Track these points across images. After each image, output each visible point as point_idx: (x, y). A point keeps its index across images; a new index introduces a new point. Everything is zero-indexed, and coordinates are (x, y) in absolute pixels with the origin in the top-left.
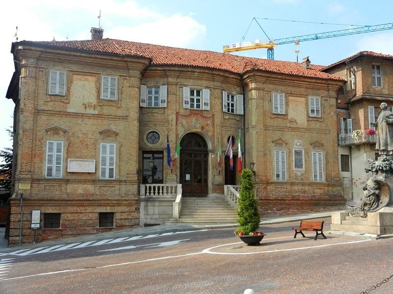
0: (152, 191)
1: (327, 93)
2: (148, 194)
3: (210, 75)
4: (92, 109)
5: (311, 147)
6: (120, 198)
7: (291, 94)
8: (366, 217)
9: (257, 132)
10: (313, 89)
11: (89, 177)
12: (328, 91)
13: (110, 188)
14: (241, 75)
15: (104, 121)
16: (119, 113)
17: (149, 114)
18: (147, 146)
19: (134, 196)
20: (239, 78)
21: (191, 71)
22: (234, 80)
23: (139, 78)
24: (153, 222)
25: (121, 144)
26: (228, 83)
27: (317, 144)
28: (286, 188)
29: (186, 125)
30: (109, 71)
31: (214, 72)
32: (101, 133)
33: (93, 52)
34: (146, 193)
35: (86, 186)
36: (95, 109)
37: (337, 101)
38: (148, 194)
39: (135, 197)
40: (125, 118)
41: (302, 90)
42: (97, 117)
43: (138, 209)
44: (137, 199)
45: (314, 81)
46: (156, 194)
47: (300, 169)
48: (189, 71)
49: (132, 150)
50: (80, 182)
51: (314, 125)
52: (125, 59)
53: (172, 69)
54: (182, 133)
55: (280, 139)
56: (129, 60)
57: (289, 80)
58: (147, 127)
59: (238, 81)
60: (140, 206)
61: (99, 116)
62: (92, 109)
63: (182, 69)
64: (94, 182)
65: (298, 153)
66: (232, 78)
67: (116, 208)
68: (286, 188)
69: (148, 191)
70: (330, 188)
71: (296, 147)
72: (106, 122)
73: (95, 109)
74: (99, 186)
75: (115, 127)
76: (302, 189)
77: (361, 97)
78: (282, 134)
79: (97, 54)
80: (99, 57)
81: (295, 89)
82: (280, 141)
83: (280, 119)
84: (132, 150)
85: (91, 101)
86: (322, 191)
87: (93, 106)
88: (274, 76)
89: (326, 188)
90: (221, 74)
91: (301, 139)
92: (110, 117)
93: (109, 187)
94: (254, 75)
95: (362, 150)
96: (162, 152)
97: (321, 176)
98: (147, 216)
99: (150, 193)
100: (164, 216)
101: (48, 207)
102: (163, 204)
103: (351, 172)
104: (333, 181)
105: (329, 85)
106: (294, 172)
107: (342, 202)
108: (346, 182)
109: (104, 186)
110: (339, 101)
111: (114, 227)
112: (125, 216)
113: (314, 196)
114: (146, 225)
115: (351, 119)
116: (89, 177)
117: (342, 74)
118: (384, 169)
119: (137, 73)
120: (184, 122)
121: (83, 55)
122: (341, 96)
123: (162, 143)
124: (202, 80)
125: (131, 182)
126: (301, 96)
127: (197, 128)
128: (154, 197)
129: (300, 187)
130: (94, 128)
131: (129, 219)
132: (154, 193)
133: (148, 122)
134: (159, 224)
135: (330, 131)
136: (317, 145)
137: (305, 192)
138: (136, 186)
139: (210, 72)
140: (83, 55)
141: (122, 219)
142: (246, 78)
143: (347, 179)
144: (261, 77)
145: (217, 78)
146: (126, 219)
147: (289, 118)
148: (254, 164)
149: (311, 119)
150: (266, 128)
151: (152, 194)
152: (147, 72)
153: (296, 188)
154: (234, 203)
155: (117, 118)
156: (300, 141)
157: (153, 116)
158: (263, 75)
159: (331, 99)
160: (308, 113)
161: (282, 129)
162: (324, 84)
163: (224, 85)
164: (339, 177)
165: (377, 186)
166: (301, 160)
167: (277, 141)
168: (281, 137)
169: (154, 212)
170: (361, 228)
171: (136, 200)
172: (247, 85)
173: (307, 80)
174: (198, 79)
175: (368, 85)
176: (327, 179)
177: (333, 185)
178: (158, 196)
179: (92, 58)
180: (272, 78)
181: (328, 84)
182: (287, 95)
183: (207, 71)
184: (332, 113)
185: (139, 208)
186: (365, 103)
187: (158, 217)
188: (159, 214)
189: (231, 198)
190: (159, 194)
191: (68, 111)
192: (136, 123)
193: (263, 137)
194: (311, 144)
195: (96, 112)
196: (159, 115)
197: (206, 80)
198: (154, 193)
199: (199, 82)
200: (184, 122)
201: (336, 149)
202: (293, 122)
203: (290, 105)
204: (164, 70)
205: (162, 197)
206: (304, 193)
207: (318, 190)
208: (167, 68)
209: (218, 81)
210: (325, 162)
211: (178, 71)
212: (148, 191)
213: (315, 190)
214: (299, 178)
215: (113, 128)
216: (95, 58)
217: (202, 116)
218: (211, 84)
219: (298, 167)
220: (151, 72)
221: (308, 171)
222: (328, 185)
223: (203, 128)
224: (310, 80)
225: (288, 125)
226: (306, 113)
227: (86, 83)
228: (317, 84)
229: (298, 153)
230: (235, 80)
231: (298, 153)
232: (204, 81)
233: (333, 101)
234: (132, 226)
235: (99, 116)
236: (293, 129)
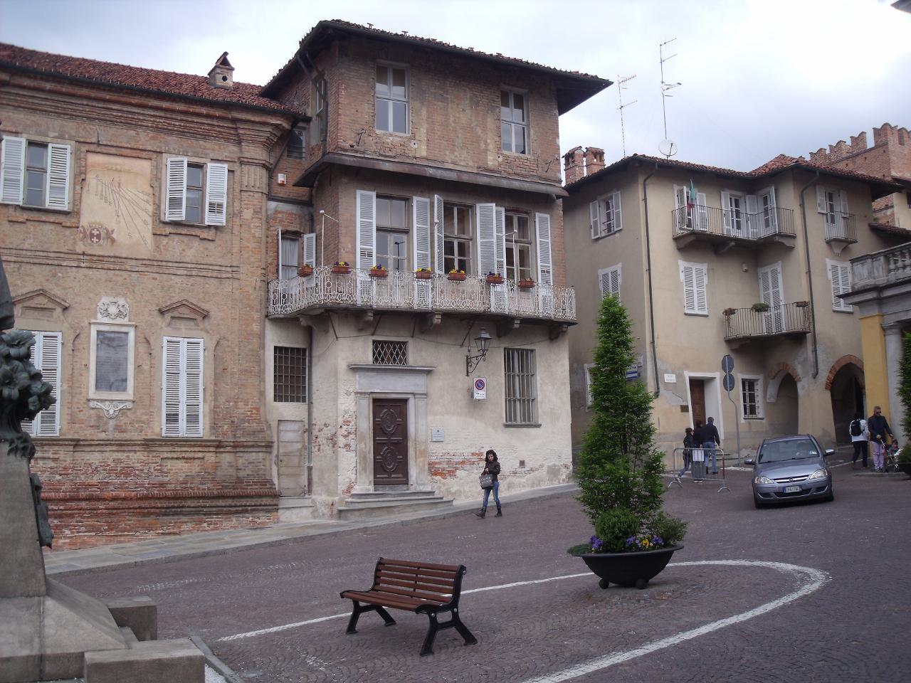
1: (234, 148)
5: (161, 322)
7: (98, 144)
12: (239, 143)
27: (185, 312)
28: (55, 460)
41: (144, 138)
51: (177, 248)
65: (107, 340)
68: (55, 460)
70: (227, 458)
71: (106, 320)
76: (117, 461)
78: (54, 275)
81: (113, 130)
82: (41, 301)
83: (47, 227)
86: (195, 467)
89: (210, 457)
91: (125, 296)
97: (193, 418)
103: (311, 403)
104: (239, 433)
106: (92, 404)
107: (265, 501)
108: (290, 435)
113: (162, 485)
115: (313, 235)
122: (287, 162)
126: (135, 153)
129: (111, 456)
135: (235, 269)
136: (186, 313)
137: (127, 472)
143: (295, 426)
147: (85, 221)
149: (168, 230)
153: (95, 458)
156: (121, 301)
159: (245, 168)
160: (159, 206)
164: (259, 422)
166: (119, 365)
167: (31, 298)
168: (48, 286)
176: (214, 426)
177: (237, 447)
182: (85, 148)
184: (247, 214)
194: (162, 312)
201: (256, 327)
202: (99, 236)
203: (91, 178)
206: (127, 475)
207: (180, 464)
210: (211, 373)
213: (169, 464)
214: (112, 423)
219: (110, 387)
221: (146, 398)
222: (219, 446)
225: (80, 248)
226: (150, 208)
229: (107, 340)
231: (112, 339)
233: (256, 177)
236: (96, 261)
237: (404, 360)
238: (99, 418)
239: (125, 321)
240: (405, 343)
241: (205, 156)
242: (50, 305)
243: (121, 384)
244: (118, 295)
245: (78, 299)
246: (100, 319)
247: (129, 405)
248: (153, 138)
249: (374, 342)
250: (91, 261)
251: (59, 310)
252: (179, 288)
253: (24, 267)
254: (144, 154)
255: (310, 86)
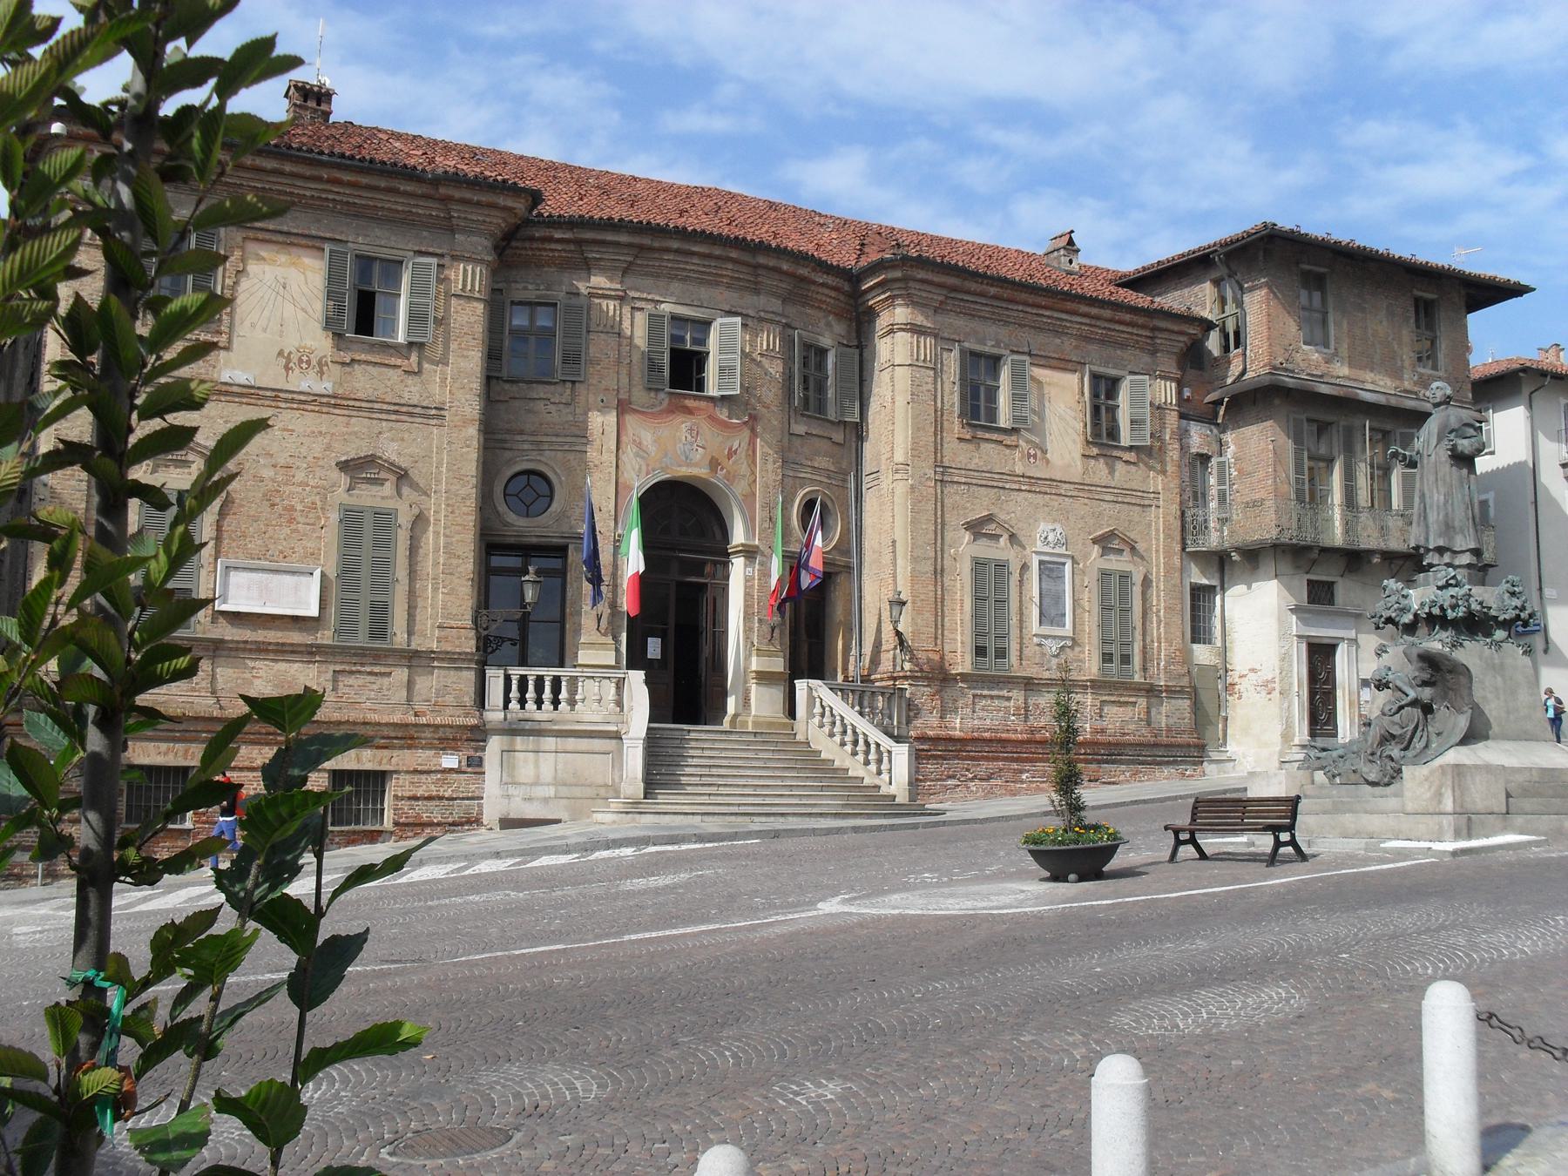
0: (531, 694)
2: (514, 705)
3: (744, 269)
4: (312, 373)
6: (412, 719)
8: (1388, 785)
9: (912, 487)
10: (1102, 342)
11: (296, 637)
12: (1153, 353)
13: (372, 679)
14: (853, 278)
15: (353, 420)
16: (411, 392)
17: (517, 403)
18: (507, 524)
19: (460, 711)
20: (847, 287)
21: (677, 251)
22: (827, 291)
23: (488, 264)
24: (532, 812)
25: (416, 511)
26: (805, 301)
27: (1115, 544)
29: (652, 449)
30: (378, 232)
31: (762, 260)
32: (344, 466)
33: (324, 158)
34: (507, 701)
35: (282, 666)
36: (321, 373)
37: (1180, 393)
38: (514, 705)
39: (467, 715)
40: (432, 413)
42: (328, 405)
43: (475, 764)
44: (473, 721)
45: (1107, 313)
46: (547, 706)
47: (1058, 631)
48: (668, 250)
49: (458, 537)
50: (261, 650)
52: (442, 190)
53: (610, 237)
54: (638, 483)
55: (990, 519)
56: (457, 194)
57: (1026, 304)
58: (508, 454)
59: (842, 298)
60: (484, 749)
61: (333, 403)
62: (312, 373)
63: (646, 241)
64: (311, 653)
66: (822, 285)
67: (395, 753)
68: (1009, 699)
69: (514, 694)
72: (359, 424)
73: (321, 373)
74: (332, 668)
75: (395, 445)
77: (1267, 380)
79: (338, 167)
80: (347, 177)
81: (1041, 338)
84: (458, 537)
85: (309, 343)
87: (314, 362)
88: (973, 286)
90: (785, 267)
92: (376, 406)
93: (370, 673)
94: (905, 279)
95: (1268, 565)
96: (561, 551)
98: (512, 790)
99: (522, 702)
100: (577, 792)
101: (144, 744)
102: (571, 743)
105: (1157, 334)
109: (352, 672)
110: (1187, 393)
111: (388, 824)
112: (427, 786)
113: (1103, 731)
114: (507, 823)
116: (296, 637)
117: (1200, 298)
118: (1451, 615)
119: (481, 245)
120: (647, 437)
121: (288, 168)
123: (563, 515)
124: (717, 284)
125: (453, 659)
127: (696, 465)
128: (538, 716)
130: (317, 449)
131: (441, 798)
132: (539, 702)
133: (509, 431)
134: (558, 821)
138: (470, 676)
139: (746, 257)
140: (288, 168)
141: (415, 798)
142: (871, 288)
144: (929, 288)
145: (768, 281)
146: (430, 798)
148: (904, 603)
150: (943, 475)
151: (531, 706)
152: (514, 244)
154: (837, 748)
155: (401, 411)
157: (529, 411)
158: (936, 279)
161: (999, 482)
162: (1143, 327)
163: (792, 310)
165: (1426, 676)
166: (1058, 599)
168: (995, 510)
169: (538, 777)
170: (1374, 822)
171: (473, 728)
172: (871, 314)
173: (1084, 309)
174: (702, 282)
175: (1287, 342)
178: (554, 715)
179: (319, 179)
180: (968, 292)
181: (1154, 329)
183: (734, 254)
185: (481, 759)
186: (1277, 402)
187: (551, 791)
188: (557, 782)
189: (821, 726)
190: (556, 708)
191: (225, 377)
192: (473, 431)
193: (931, 506)
195: (325, 386)
196: (552, 408)
197: (729, 286)
198: (539, 702)
199: (704, 293)
200: (647, 437)
204: (579, 242)
205: (569, 716)
208: (589, 235)
209: (774, 295)
211: (630, 245)
212: (514, 694)
215: (390, 450)
216: (329, 181)
217: (712, 419)
218: (751, 302)
220: (527, 245)
223: (714, 464)
224: (1094, 311)
225: (1019, 469)
227: (294, 276)
228: (1117, 327)
230: (833, 294)
231: (1051, 570)
232: (721, 289)
234: (454, 824)
235: (333, 403)
237: (1331, 602)
238: (1044, 655)
239: (1063, 551)
240: (1333, 583)
241: (1124, 368)
242: (998, 532)
243: (1058, 620)
244: (1055, 521)
245: (1020, 525)
246: (1040, 547)
247: (1069, 643)
248: (1076, 347)
249: (1310, 582)
250: (1031, 484)
251: (1006, 536)
252: (1110, 517)
253: (973, 488)
254: (1070, 366)
255: (1208, 286)
